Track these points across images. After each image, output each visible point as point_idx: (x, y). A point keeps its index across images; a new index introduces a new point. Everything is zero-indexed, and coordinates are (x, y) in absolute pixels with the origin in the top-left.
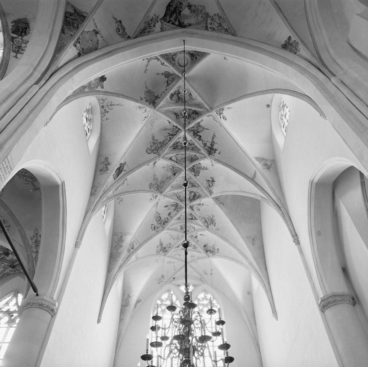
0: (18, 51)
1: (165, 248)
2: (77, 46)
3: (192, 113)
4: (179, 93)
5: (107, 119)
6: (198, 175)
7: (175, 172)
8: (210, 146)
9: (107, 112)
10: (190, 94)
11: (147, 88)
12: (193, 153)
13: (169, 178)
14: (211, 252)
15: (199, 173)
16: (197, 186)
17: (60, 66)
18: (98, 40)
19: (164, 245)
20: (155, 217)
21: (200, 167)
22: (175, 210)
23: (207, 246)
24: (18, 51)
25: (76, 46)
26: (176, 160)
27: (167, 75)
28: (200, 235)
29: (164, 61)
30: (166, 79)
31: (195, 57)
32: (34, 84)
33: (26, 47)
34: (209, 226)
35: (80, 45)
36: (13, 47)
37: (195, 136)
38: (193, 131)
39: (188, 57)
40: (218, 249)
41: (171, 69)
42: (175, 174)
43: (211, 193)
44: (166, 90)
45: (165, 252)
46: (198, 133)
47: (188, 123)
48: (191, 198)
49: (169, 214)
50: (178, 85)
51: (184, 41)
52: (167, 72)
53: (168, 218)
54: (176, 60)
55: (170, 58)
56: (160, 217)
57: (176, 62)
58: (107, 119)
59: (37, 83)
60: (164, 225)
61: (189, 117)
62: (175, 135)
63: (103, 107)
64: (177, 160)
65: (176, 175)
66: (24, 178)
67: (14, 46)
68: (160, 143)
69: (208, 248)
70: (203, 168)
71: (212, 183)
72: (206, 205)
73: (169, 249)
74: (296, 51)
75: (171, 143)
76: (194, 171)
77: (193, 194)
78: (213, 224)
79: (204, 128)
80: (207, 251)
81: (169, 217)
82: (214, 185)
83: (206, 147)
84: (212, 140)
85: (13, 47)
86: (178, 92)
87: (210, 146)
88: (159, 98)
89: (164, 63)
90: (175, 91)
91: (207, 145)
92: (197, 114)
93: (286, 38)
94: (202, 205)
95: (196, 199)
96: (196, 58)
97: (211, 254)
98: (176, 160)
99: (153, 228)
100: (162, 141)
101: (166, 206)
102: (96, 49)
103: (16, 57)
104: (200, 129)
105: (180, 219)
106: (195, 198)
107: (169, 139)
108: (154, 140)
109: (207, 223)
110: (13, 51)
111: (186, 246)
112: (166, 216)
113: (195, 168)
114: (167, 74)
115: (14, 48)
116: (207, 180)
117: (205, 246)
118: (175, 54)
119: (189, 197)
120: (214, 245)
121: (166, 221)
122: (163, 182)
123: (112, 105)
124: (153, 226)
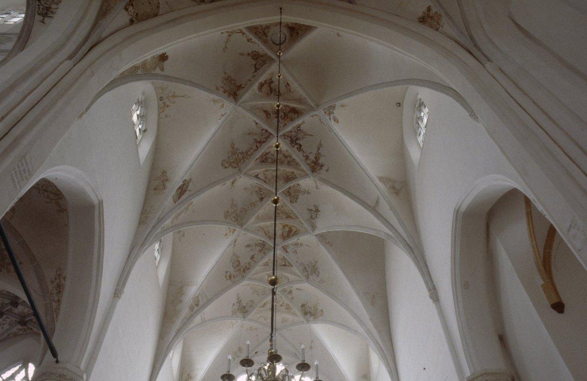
0: (46, 13)
2: (130, 10)
3: (289, 112)
4: (272, 82)
5: (166, 116)
8: (314, 160)
10: (288, 84)
11: (225, 73)
12: (289, 170)
13: (253, 205)
14: (311, 314)
15: (297, 199)
16: (293, 217)
17: (103, 36)
18: (159, 3)
19: (244, 304)
20: (231, 262)
21: (299, 191)
22: (260, 251)
23: (306, 306)
24: (46, 13)
25: (127, 10)
26: (264, 179)
27: (256, 56)
29: (251, 36)
30: (254, 62)
31: (296, 31)
32: (66, 59)
33: (57, 8)
34: (311, 277)
35: (133, 8)
36: (39, 8)
37: (293, 145)
38: (291, 137)
39: (285, 31)
41: (260, 47)
42: (262, 199)
43: (314, 227)
44: (254, 77)
46: (297, 140)
47: (283, 126)
48: (285, 235)
49: (252, 257)
50: (269, 71)
51: (281, 9)
52: (256, 52)
53: (250, 263)
54: (269, 34)
55: (260, 32)
57: (269, 38)
59: (70, 58)
62: (264, 142)
64: (266, 178)
65: (264, 200)
66: (46, 194)
67: (41, 7)
68: (242, 153)
72: (306, 245)
74: (437, 26)
75: (259, 154)
76: (290, 195)
77: (287, 229)
78: (315, 273)
79: (306, 134)
80: (305, 313)
82: (318, 216)
83: (308, 162)
85: (39, 8)
87: (314, 160)
88: (243, 88)
89: (251, 39)
90: (265, 79)
91: (310, 158)
92: (296, 112)
93: (424, 9)
95: (292, 236)
96: (298, 33)
97: (312, 318)
98: (264, 179)
99: (228, 277)
100: (244, 150)
101: (248, 246)
102: (156, 15)
103: (43, 22)
104: (300, 135)
105: (267, 265)
108: (233, 148)
109: (307, 271)
110: (39, 14)
111: (273, 283)
113: (291, 191)
114: (255, 55)
115: (41, 9)
117: (303, 306)
118: (268, 27)
120: (317, 305)
122: (245, 209)
123: (174, 96)
124: (228, 274)
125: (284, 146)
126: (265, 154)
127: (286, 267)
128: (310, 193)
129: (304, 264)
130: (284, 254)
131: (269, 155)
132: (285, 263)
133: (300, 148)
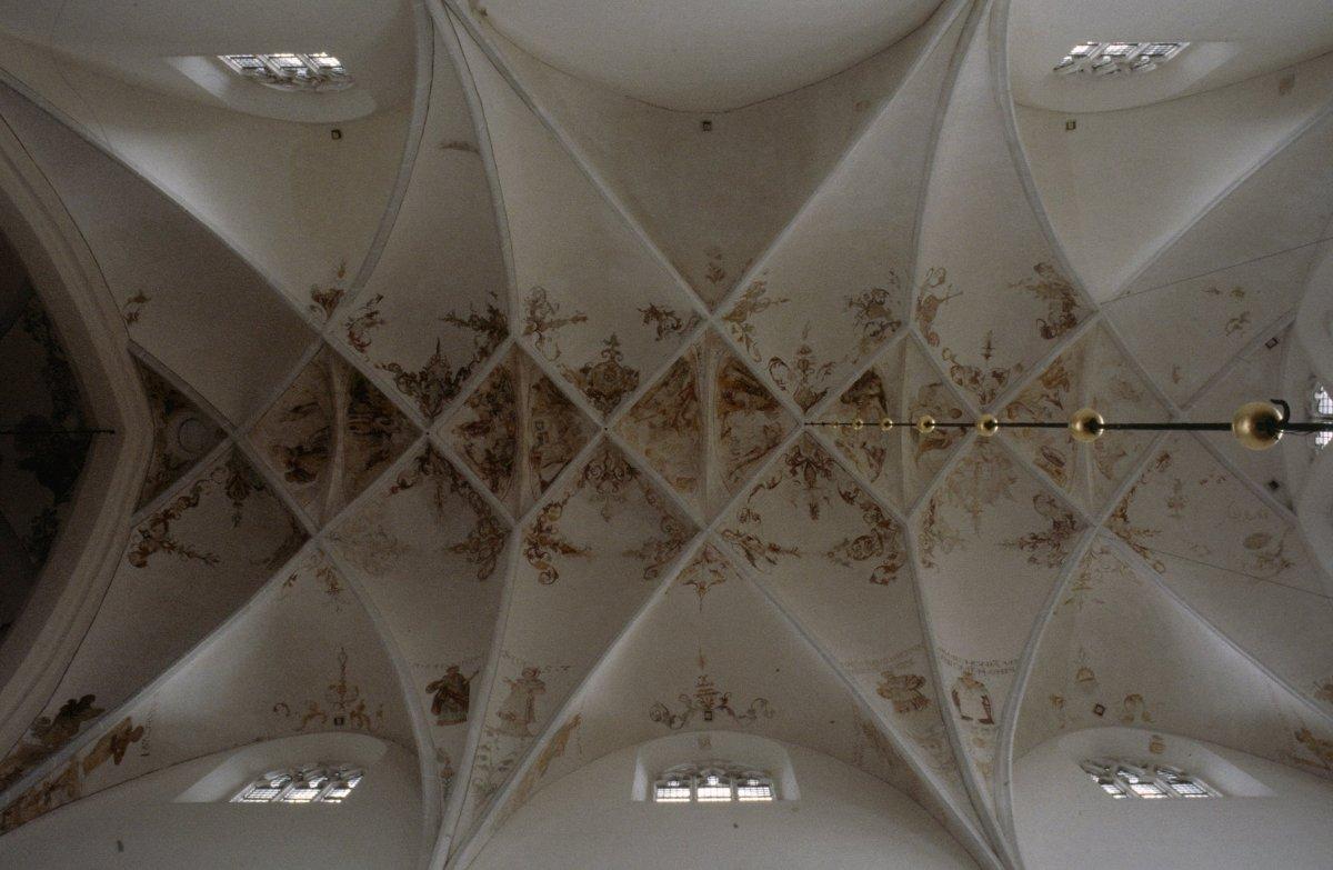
1: (1057, 525)
4: (300, 448)
5: (380, 714)
6: (637, 375)
7: (625, 467)
8: (487, 332)
9: (362, 707)
10: (297, 409)
12: (527, 400)
13: (650, 493)
14: (1069, 304)
16: (687, 380)
19: (1044, 526)
20: (846, 564)
22: (827, 474)
23: (1049, 324)
26: (562, 465)
28: (987, 356)
30: (253, 491)
31: (166, 397)
40: (1038, 268)
42: (633, 471)
44: (274, 495)
45: (1073, 523)
48: (760, 401)
49: (848, 498)
52: (228, 488)
56: (857, 542)
58: (380, 714)
60: (891, 527)
61: (386, 416)
63: (339, 721)
68: (480, 524)
69: (1058, 315)
70: (612, 358)
71: (664, 317)
73: (1059, 504)
75: (481, 484)
77: (740, 396)
78: (882, 303)
79: (436, 359)
80: (1071, 322)
81: (859, 500)
83: (490, 349)
84: (467, 325)
86: (296, 453)
87: (487, 332)
92: (361, 388)
94: (806, 352)
97: (1078, 300)
98: (562, 465)
99: (888, 576)
101: (814, 511)
104: (440, 373)
105: (883, 451)
106: (754, 383)
107: (467, 491)
109: (883, 328)
112: (855, 512)
113: (608, 388)
114: (238, 489)
116: (657, 340)
119: (760, 409)
121: (874, 512)
123: (342, 690)
124: (880, 575)
125: (459, 412)
126: (491, 463)
127: (888, 397)
128: (614, 337)
129: (864, 340)
130: (832, 400)
131: (498, 453)
132: (872, 396)
133: (465, 373)
